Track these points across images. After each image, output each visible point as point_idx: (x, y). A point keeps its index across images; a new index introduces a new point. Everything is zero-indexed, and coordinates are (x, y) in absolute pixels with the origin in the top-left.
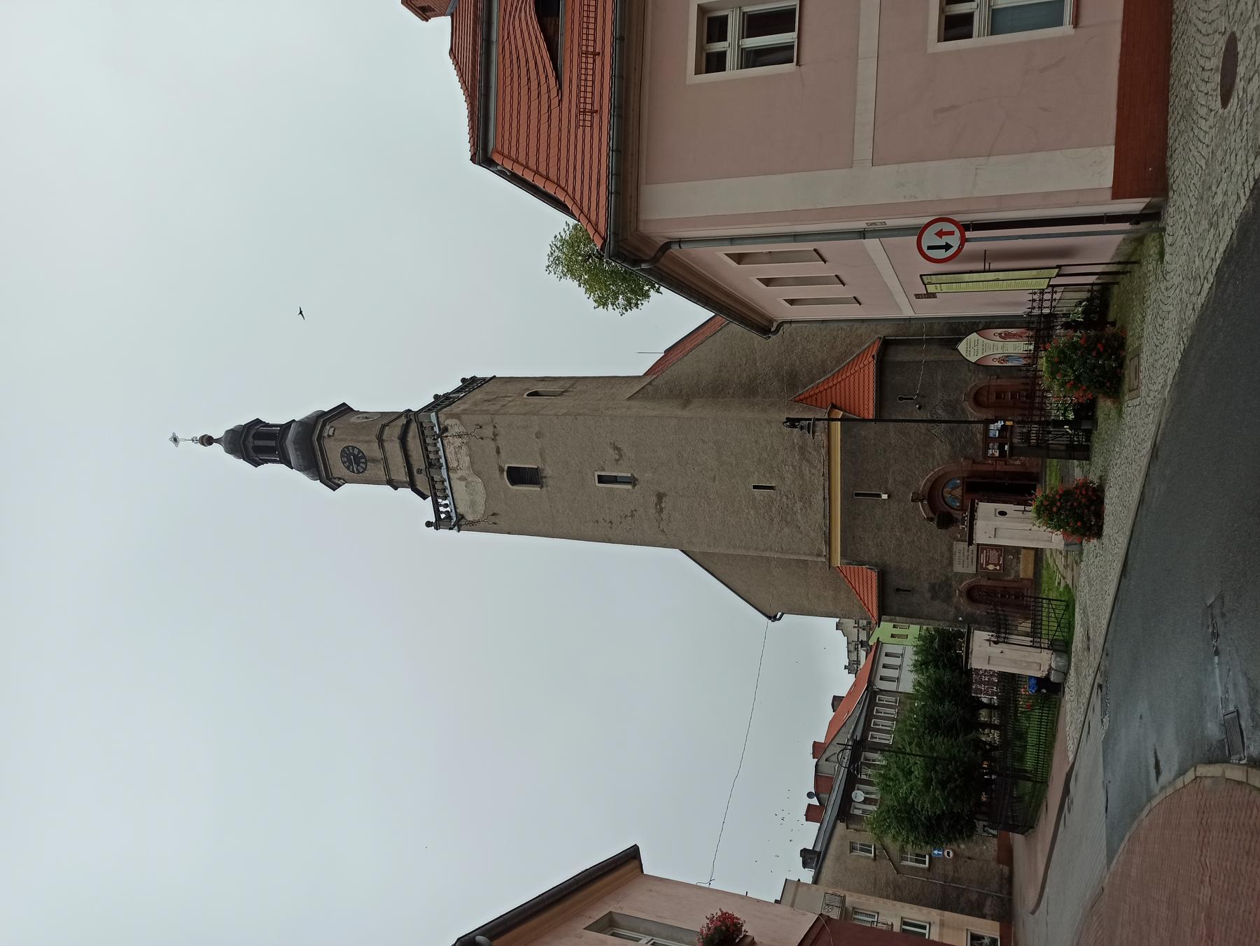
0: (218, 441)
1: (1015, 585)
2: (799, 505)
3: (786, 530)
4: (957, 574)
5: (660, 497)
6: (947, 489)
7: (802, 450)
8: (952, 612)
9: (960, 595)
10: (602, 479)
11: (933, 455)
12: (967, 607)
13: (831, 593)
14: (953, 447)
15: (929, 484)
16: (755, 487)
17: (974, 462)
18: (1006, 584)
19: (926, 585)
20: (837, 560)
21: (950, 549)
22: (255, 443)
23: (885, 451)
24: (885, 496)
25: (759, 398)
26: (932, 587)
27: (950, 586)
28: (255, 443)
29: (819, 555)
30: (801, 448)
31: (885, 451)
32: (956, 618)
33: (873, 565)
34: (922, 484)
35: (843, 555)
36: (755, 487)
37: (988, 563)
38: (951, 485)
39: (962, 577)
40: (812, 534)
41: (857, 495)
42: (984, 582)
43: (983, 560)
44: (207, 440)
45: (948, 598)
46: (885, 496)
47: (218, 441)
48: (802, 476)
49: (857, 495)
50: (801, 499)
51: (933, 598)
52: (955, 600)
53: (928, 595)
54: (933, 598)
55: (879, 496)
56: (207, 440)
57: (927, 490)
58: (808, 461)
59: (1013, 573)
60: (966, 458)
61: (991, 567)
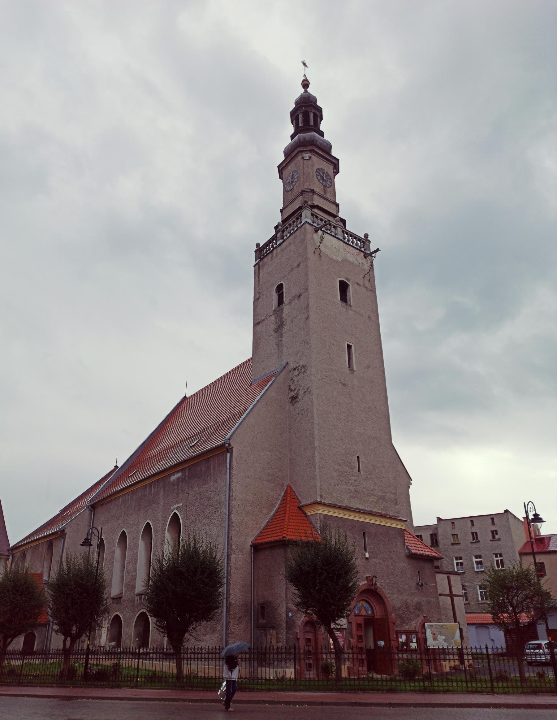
0: (306, 91)
3: (335, 474)
5: (344, 385)
7: (383, 498)
10: (349, 347)
14: (399, 609)
22: (307, 113)
23: (392, 558)
28: (307, 113)
40: (335, 494)
41: (364, 533)
44: (306, 84)
47: (306, 91)
49: (364, 533)
50: (356, 491)
56: (306, 84)
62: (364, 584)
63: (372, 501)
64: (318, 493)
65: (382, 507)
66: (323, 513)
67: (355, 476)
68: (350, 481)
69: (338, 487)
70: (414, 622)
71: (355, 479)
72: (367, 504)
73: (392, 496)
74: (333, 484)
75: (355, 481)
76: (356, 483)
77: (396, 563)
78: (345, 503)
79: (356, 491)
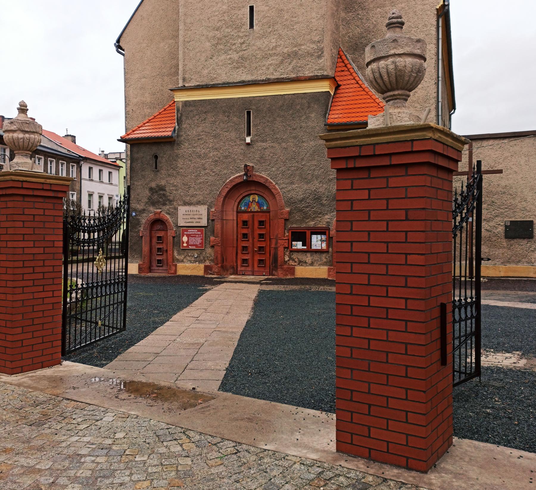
1: (170, 260)
2: (235, 56)
3: (208, 44)
4: (176, 209)
6: (257, 198)
7: (294, 55)
8: (140, 207)
9: (156, 213)
11: (292, 183)
12: (144, 219)
13: (148, 100)
14: (301, 201)
15: (262, 181)
16: (252, 8)
17: (286, 220)
18: (170, 252)
19: (163, 183)
20: (181, 97)
21: (199, 203)
23: (295, 138)
24: (248, 140)
25: (343, 14)
26: (162, 188)
27: (164, 204)
29: (184, 80)
30: (296, 53)
31: (295, 138)
32: (135, 210)
33: (178, 132)
34: (262, 174)
35: (186, 104)
36: (252, 8)
37: (188, 236)
38: (262, 201)
39: (174, 214)
40: (205, 72)
41: (249, 113)
42: (171, 233)
43: (191, 231)
45: (153, 203)
46: (248, 140)
48: (266, 57)
49: (249, 113)
51: (151, 189)
52: (152, 209)
53: (153, 185)
54: (151, 189)
55: (249, 134)
57: (255, 179)
58: (282, 62)
59: (181, 257)
60: (290, 213)
61: (185, 239)
62: (240, 176)
63: (271, 65)
64: (180, 77)
65: (290, 68)
66: (181, 100)
67: (242, 37)
68: (234, 47)
69: (212, 60)
70: (327, 217)
71: (242, 40)
72: (261, 71)
73: (314, 46)
74: (203, 59)
75: (243, 43)
76: (244, 46)
77: (303, 142)
78: (223, 78)
79: (242, 58)
